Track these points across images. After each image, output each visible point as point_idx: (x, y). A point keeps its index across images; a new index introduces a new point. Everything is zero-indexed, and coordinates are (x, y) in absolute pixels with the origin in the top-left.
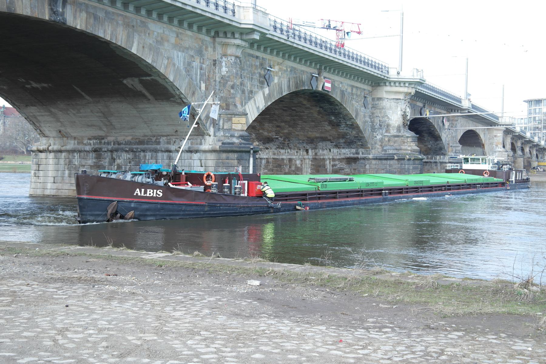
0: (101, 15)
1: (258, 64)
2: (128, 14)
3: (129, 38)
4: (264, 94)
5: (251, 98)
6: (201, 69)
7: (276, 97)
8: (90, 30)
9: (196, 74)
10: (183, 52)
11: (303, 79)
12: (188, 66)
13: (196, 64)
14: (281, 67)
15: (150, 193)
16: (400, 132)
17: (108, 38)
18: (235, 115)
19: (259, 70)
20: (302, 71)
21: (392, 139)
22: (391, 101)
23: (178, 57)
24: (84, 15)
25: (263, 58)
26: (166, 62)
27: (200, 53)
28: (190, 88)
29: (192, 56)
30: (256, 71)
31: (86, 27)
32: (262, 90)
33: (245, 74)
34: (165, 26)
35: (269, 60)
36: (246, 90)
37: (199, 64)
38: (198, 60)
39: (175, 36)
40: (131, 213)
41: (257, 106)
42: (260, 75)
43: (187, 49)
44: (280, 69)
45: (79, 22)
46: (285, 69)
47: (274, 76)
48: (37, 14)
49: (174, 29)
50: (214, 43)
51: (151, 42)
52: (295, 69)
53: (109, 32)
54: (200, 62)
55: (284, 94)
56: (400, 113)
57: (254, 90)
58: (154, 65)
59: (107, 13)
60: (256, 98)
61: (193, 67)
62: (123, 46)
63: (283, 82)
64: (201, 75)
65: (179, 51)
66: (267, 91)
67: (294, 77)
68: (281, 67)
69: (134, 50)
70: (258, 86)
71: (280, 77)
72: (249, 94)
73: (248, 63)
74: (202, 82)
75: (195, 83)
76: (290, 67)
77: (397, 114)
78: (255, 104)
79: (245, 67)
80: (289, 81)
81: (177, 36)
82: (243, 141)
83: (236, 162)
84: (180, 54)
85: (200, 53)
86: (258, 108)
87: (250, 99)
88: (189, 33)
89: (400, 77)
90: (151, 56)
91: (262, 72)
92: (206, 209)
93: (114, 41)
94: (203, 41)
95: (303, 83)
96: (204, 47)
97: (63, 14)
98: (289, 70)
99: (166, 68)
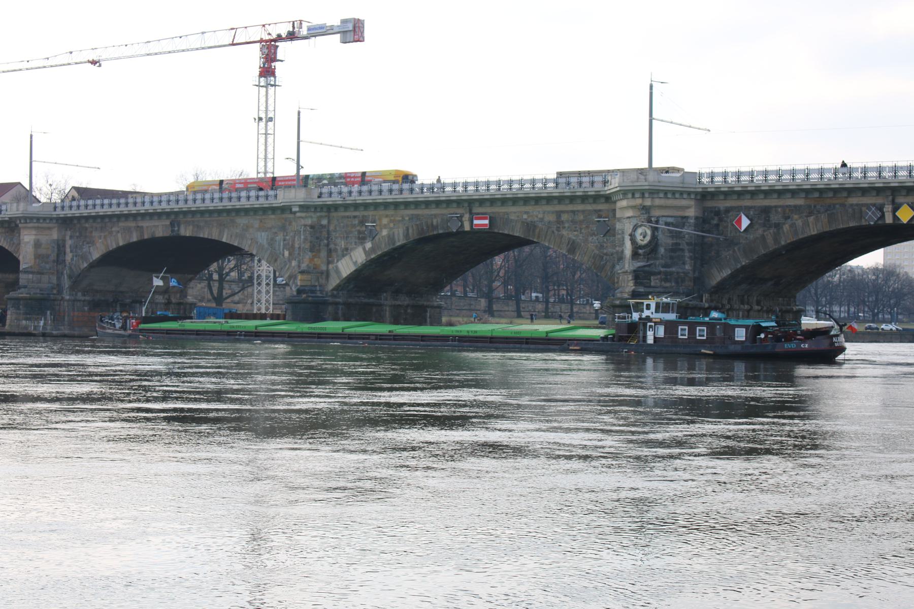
0: (202, 224)
1: (356, 222)
3: (221, 233)
4: (364, 249)
5: (346, 255)
6: (284, 240)
7: (384, 248)
8: (195, 235)
9: (279, 245)
10: (266, 231)
11: (435, 223)
12: (271, 242)
13: (279, 237)
14: (392, 218)
17: (206, 236)
19: (358, 228)
20: (432, 215)
23: (261, 236)
24: (191, 227)
25: (363, 216)
26: (249, 242)
27: (283, 228)
29: (276, 233)
30: (354, 230)
32: (362, 245)
33: (337, 235)
35: (372, 215)
36: (338, 248)
37: (282, 237)
38: (282, 235)
41: (354, 260)
42: (359, 232)
43: (270, 228)
44: (391, 221)
45: (188, 232)
46: (401, 219)
47: (381, 229)
51: (238, 231)
52: (418, 215)
53: (207, 233)
54: (284, 236)
55: (398, 244)
57: (350, 247)
58: (240, 246)
60: (352, 254)
61: (276, 241)
62: (217, 239)
63: (396, 233)
64: (284, 245)
65: (263, 231)
66: (369, 245)
67: (417, 225)
68: (392, 218)
69: (224, 240)
70: (356, 242)
71: (391, 229)
72: (343, 251)
73: (342, 224)
74: (285, 250)
75: (278, 252)
76: (408, 215)
79: (338, 229)
80: (408, 229)
81: (261, 221)
84: (263, 234)
85: (283, 228)
86: (355, 263)
87: (343, 256)
88: (273, 216)
93: (210, 238)
95: (436, 227)
96: (287, 223)
97: (178, 230)
98: (407, 218)
99: (250, 246)
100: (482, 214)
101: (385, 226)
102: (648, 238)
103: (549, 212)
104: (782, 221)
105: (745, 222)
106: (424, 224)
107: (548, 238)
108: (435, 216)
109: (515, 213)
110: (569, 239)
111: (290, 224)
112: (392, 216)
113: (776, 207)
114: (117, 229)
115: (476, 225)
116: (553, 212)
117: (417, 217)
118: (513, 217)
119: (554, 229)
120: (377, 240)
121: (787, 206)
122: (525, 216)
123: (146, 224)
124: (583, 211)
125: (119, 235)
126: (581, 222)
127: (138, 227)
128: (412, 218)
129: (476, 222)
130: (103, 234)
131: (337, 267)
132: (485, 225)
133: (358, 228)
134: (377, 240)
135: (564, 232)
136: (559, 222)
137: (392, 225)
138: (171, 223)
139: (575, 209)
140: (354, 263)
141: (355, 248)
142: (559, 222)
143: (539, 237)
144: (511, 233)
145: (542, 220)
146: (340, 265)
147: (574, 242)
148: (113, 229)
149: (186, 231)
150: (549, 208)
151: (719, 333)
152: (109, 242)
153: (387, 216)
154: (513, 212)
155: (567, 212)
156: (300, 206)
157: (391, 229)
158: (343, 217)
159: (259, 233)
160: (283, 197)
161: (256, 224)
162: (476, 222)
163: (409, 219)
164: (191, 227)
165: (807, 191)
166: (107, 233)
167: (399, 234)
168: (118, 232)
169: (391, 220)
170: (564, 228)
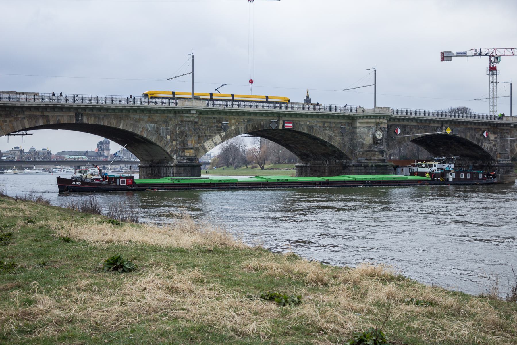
1: (215, 121)
2: (117, 114)
4: (221, 136)
5: (209, 139)
6: (167, 129)
8: (96, 123)
9: (163, 132)
15: (77, 183)
16: (371, 148)
17: (106, 125)
18: (186, 149)
19: (216, 124)
20: (260, 120)
21: (365, 153)
22: (365, 128)
23: (150, 126)
24: (93, 118)
25: (219, 118)
27: (166, 122)
28: (159, 139)
31: (94, 122)
34: (140, 114)
35: (225, 118)
38: (165, 126)
39: (148, 117)
40: (72, 190)
41: (215, 142)
48: (70, 122)
49: (147, 115)
50: (176, 116)
56: (371, 136)
58: (134, 131)
59: (105, 115)
60: (213, 138)
61: (161, 129)
62: (114, 126)
63: (240, 128)
65: (151, 123)
69: (121, 127)
73: (206, 122)
76: (247, 119)
77: (369, 137)
78: (213, 142)
79: (203, 124)
81: (149, 117)
82: (188, 161)
83: (183, 172)
84: (151, 125)
87: (207, 139)
89: (364, 113)
90: (132, 128)
91: (220, 125)
92: (97, 189)
94: (168, 117)
97: (82, 120)
98: (246, 121)
99: (141, 132)
100: (291, 121)
101: (233, 124)
102: (381, 136)
103: (319, 122)
104: (410, 131)
105: (399, 131)
106: (256, 124)
107: (319, 134)
108: (262, 120)
109: (303, 121)
110: (329, 135)
111: (171, 120)
112: (238, 119)
113: (408, 125)
114: (23, 116)
115: (286, 126)
116: (321, 122)
117: (252, 120)
118: (302, 123)
119: (322, 130)
120: (229, 132)
121: (412, 125)
122: (308, 123)
123: (50, 114)
124: (335, 122)
125: (26, 121)
126: (334, 127)
127: (44, 115)
128: (249, 121)
129: (286, 125)
130: (8, 120)
131: (203, 145)
132: (291, 126)
133: (216, 124)
134: (229, 132)
135: (326, 132)
136: (324, 127)
137: (237, 124)
138: (75, 114)
139: (331, 121)
140: (214, 143)
141: (216, 135)
142: (324, 127)
143: (315, 133)
144: (302, 131)
145: (316, 125)
146: (205, 144)
147: (331, 136)
148: (19, 116)
149: (88, 120)
150: (319, 120)
151: (475, 176)
152: (15, 124)
153: (234, 119)
154: (303, 121)
155: (327, 122)
156: (197, 111)
157: (237, 126)
158: (207, 118)
159: (148, 124)
160: (181, 105)
161: (146, 119)
162: (286, 125)
163: (247, 121)
164: (93, 118)
165: (417, 120)
166: (12, 119)
167: (241, 129)
168: (24, 118)
169: (237, 121)
170: (326, 129)
